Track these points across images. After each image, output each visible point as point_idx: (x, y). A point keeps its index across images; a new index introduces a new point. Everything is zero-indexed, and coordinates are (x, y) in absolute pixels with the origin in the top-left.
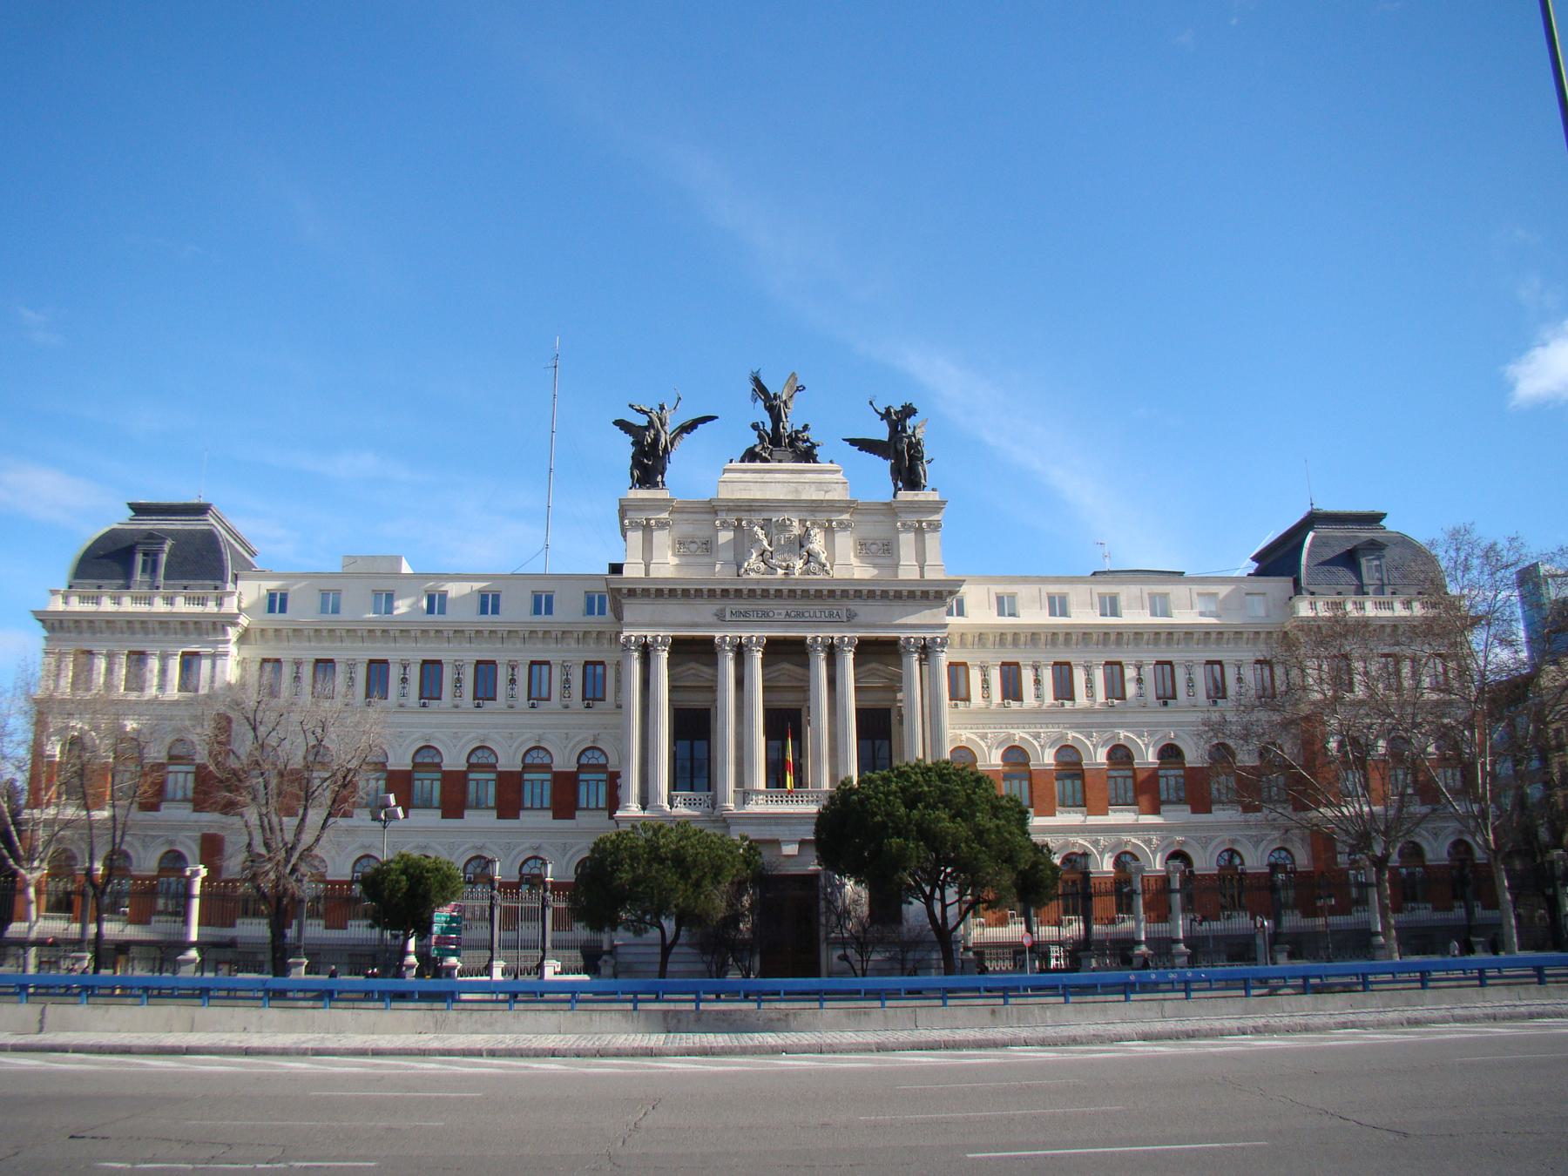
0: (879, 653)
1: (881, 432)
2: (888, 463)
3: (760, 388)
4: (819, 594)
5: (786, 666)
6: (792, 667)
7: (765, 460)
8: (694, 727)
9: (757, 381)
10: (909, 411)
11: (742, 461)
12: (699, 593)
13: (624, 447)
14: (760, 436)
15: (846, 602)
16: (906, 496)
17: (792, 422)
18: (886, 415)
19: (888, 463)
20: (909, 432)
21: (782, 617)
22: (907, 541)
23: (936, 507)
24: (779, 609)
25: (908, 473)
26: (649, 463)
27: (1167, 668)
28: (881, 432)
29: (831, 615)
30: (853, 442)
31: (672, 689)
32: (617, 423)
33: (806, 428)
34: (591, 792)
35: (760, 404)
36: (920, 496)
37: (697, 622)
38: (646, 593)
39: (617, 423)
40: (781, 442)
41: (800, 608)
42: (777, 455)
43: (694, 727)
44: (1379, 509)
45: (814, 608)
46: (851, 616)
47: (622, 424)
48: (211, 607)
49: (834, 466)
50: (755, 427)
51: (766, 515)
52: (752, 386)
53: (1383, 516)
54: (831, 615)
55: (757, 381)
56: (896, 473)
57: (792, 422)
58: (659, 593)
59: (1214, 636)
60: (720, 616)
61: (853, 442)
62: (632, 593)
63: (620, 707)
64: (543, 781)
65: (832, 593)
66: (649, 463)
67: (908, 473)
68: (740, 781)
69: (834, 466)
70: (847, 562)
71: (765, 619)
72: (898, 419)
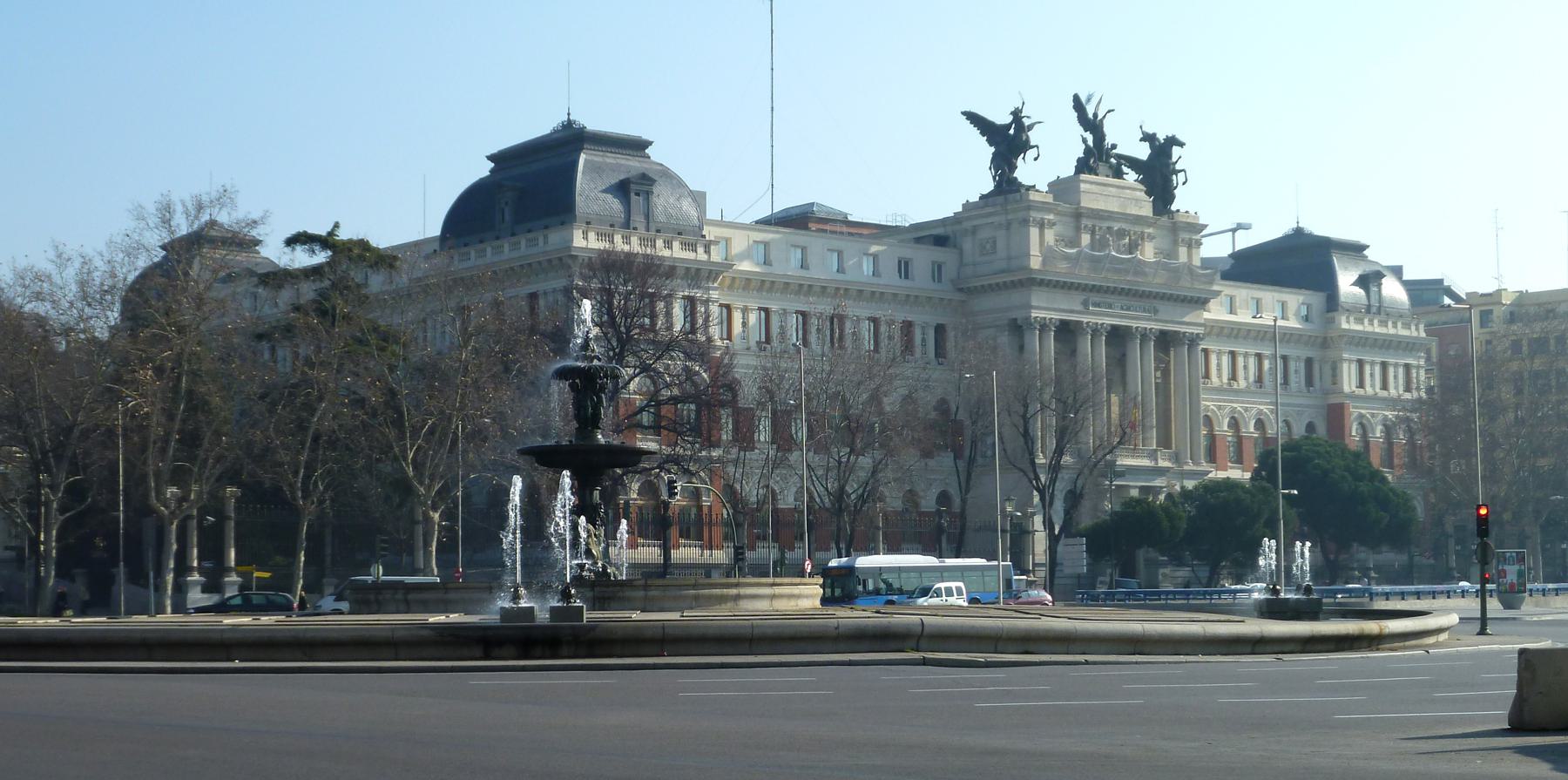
0: (1166, 341)
1: (1143, 152)
10: (1172, 141)
18: (1149, 138)
28: (1143, 152)
32: (964, 113)
39: (964, 113)
44: (1363, 241)
47: (974, 118)
50: (1085, 141)
57: (1109, 141)
60: (1085, 304)
62: (1042, 283)
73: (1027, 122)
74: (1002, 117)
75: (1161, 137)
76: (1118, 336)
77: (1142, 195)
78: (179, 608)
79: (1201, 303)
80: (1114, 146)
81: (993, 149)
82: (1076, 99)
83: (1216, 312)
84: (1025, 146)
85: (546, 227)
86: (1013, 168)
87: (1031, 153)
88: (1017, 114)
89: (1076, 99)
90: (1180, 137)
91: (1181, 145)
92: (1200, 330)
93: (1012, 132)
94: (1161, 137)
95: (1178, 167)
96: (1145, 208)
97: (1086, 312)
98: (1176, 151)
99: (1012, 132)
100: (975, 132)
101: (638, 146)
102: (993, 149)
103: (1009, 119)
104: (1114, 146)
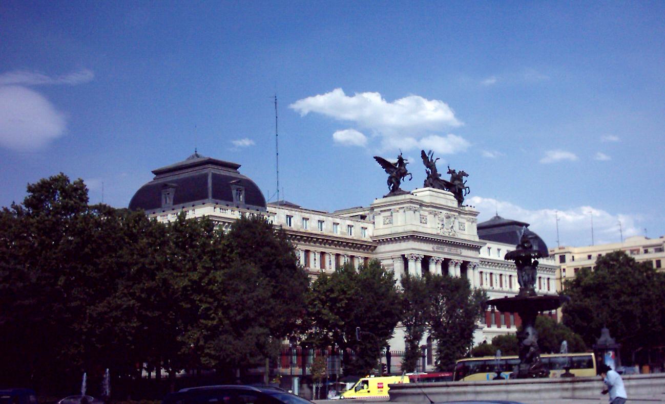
1: (447, 178)
7: (433, 187)
10: (463, 174)
20: (463, 182)
24: (446, 249)
32: (375, 158)
39: (375, 158)
40: (433, 180)
44: (528, 223)
47: (380, 160)
50: (428, 173)
51: (440, 211)
53: (529, 225)
57: (438, 173)
73: (405, 162)
74: (393, 161)
75: (457, 172)
77: (453, 198)
78: (424, 370)
79: (477, 248)
80: (440, 175)
81: (389, 175)
82: (423, 152)
83: (483, 253)
84: (404, 174)
85: (193, 206)
86: (399, 183)
87: (407, 178)
88: (401, 160)
89: (423, 152)
90: (467, 173)
91: (467, 175)
92: (477, 261)
93: (397, 166)
94: (457, 172)
95: (465, 185)
96: (455, 204)
97: (434, 252)
98: (464, 178)
99: (397, 166)
101: (235, 167)
102: (389, 175)
103: (396, 161)
104: (440, 175)
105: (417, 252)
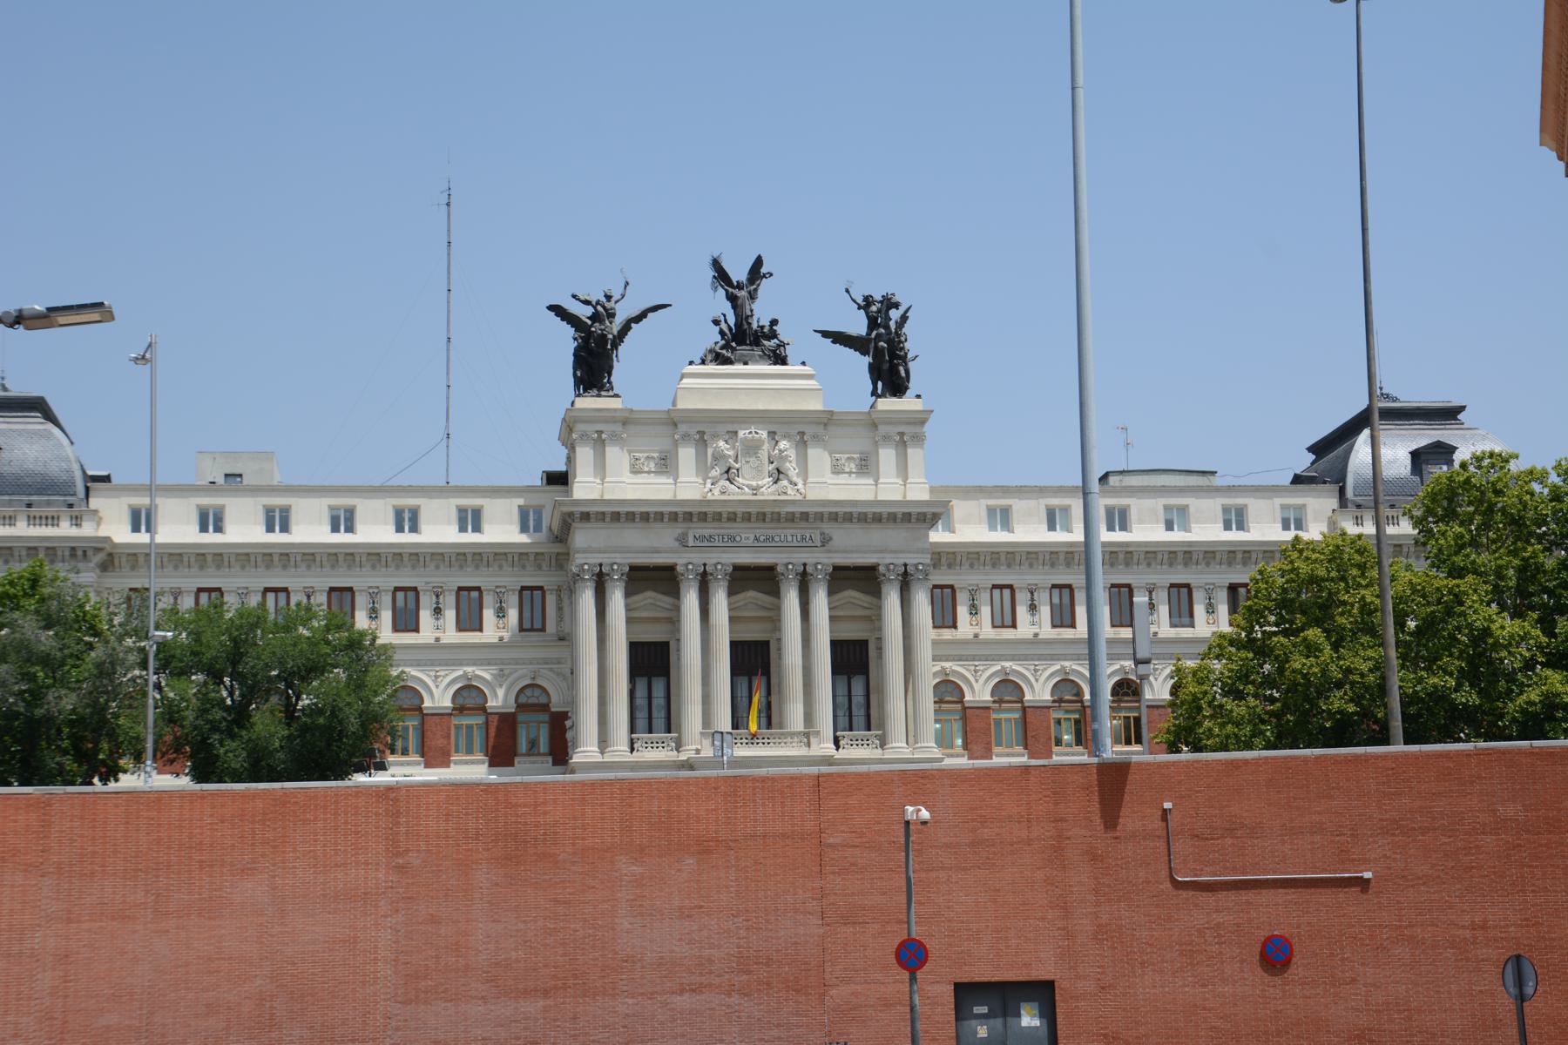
0: (858, 580)
1: (857, 325)
2: (867, 360)
3: (722, 276)
4: (791, 518)
5: (751, 594)
6: (760, 595)
7: (731, 363)
8: (652, 662)
9: (716, 264)
10: (889, 303)
11: (703, 362)
12: (660, 517)
13: (565, 339)
14: (722, 333)
15: (819, 524)
16: (888, 404)
17: (761, 314)
19: (867, 360)
21: (750, 543)
22: (887, 456)
23: (920, 419)
24: (747, 535)
25: (890, 373)
26: (593, 363)
27: (1184, 590)
28: (857, 325)
29: (803, 539)
30: (825, 334)
31: (629, 621)
32: (551, 308)
33: (774, 322)
34: (532, 731)
35: (721, 293)
36: (906, 404)
37: (655, 546)
38: (602, 517)
39: (551, 308)
40: (745, 339)
41: (770, 532)
42: (743, 350)
43: (652, 662)
44: (1456, 403)
45: (788, 533)
46: (826, 540)
47: (558, 310)
48: (65, 529)
49: (807, 370)
50: (716, 322)
52: (711, 273)
53: (1462, 408)
54: (803, 539)
55: (716, 264)
56: (876, 372)
58: (616, 517)
59: (1240, 556)
60: (682, 541)
61: (825, 334)
62: (586, 517)
63: (566, 638)
64: (470, 727)
65: (805, 516)
66: (593, 363)
67: (890, 373)
68: (707, 722)
69: (807, 370)
70: (825, 481)
71: (732, 542)
72: (879, 311)
74: (584, 312)
76: (756, 580)
90: (896, 299)
100: (570, 331)
105: (595, 559)
